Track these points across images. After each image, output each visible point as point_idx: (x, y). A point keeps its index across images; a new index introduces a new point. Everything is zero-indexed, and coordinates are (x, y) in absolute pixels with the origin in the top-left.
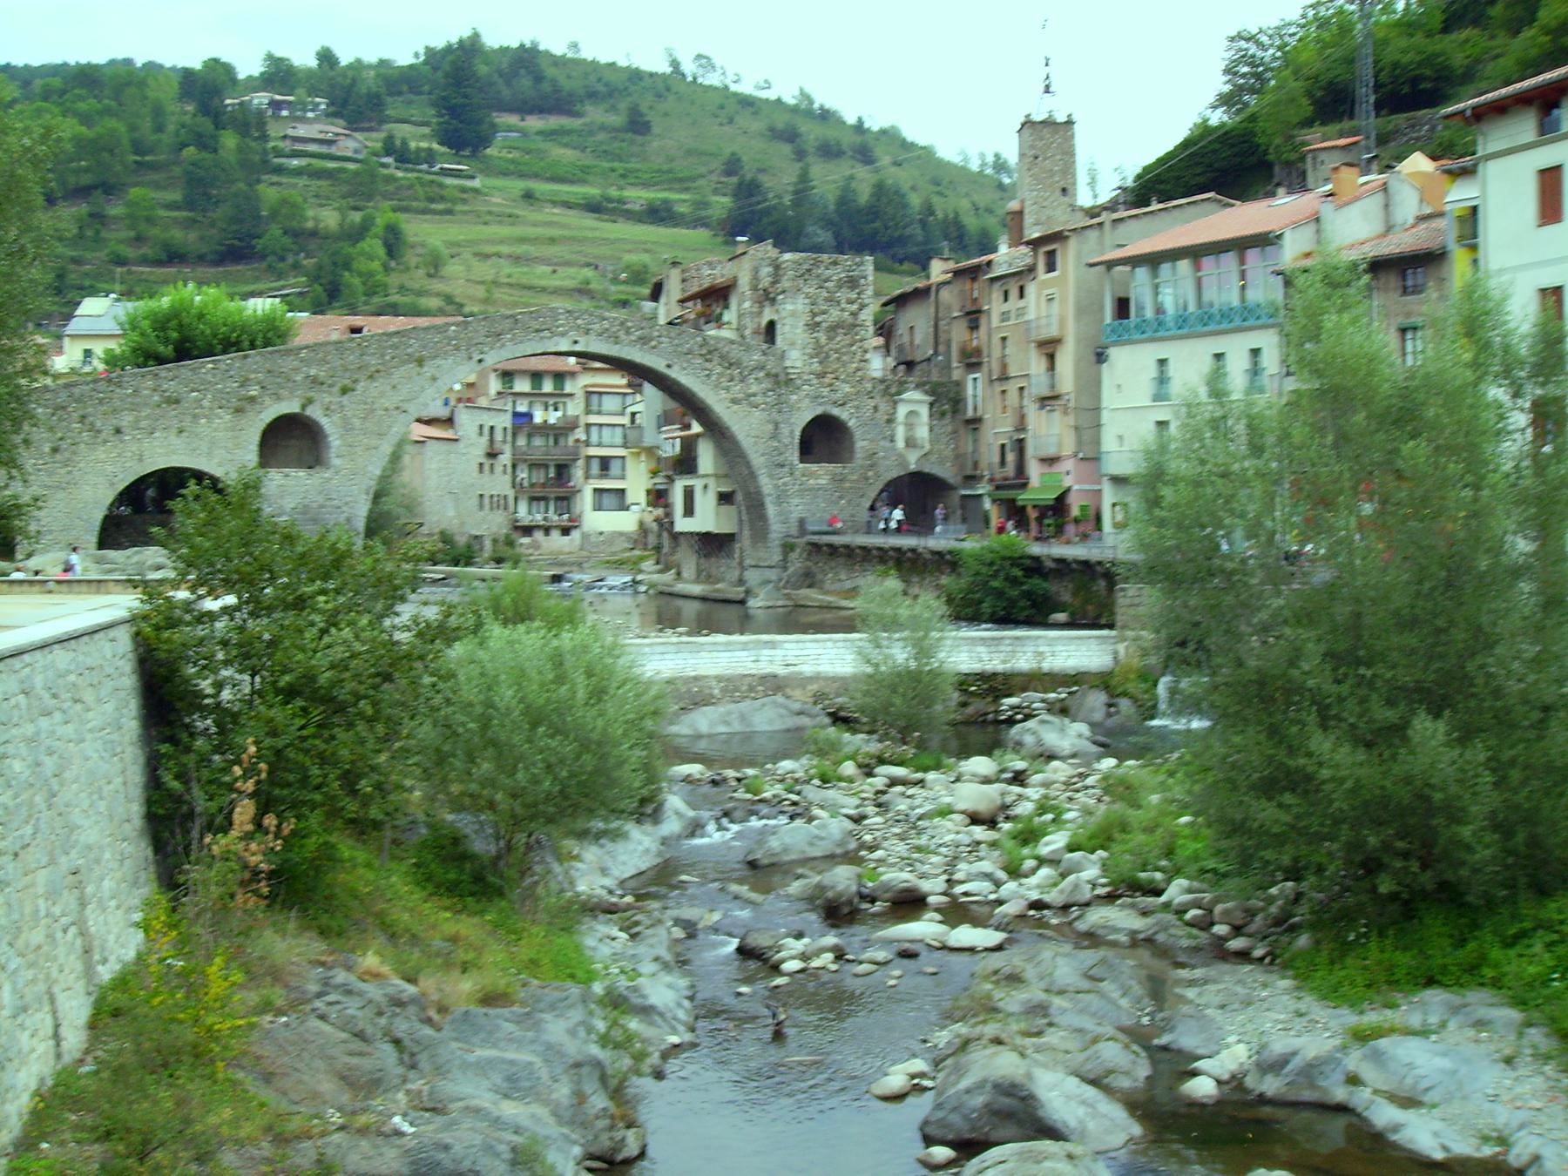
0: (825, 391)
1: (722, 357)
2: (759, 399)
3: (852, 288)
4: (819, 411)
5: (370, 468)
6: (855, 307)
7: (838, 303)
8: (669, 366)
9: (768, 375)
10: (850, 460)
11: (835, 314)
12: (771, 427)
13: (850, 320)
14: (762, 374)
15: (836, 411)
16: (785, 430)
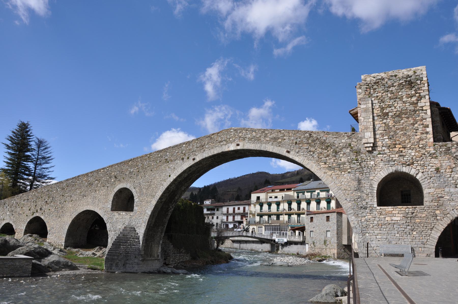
0: (396, 157)
1: (322, 143)
2: (347, 166)
3: (411, 88)
4: (391, 170)
5: (147, 211)
6: (414, 99)
7: (401, 99)
8: (288, 152)
9: (352, 150)
10: (420, 202)
11: (399, 105)
12: (356, 183)
13: (412, 108)
14: (348, 151)
15: (405, 169)
16: (365, 184)
